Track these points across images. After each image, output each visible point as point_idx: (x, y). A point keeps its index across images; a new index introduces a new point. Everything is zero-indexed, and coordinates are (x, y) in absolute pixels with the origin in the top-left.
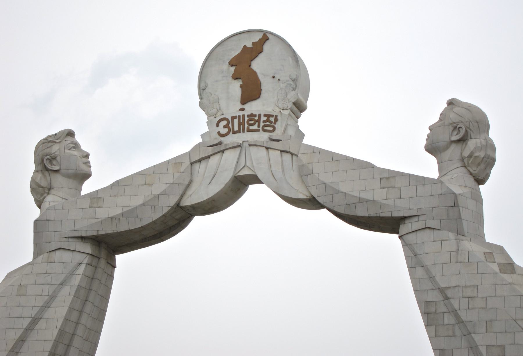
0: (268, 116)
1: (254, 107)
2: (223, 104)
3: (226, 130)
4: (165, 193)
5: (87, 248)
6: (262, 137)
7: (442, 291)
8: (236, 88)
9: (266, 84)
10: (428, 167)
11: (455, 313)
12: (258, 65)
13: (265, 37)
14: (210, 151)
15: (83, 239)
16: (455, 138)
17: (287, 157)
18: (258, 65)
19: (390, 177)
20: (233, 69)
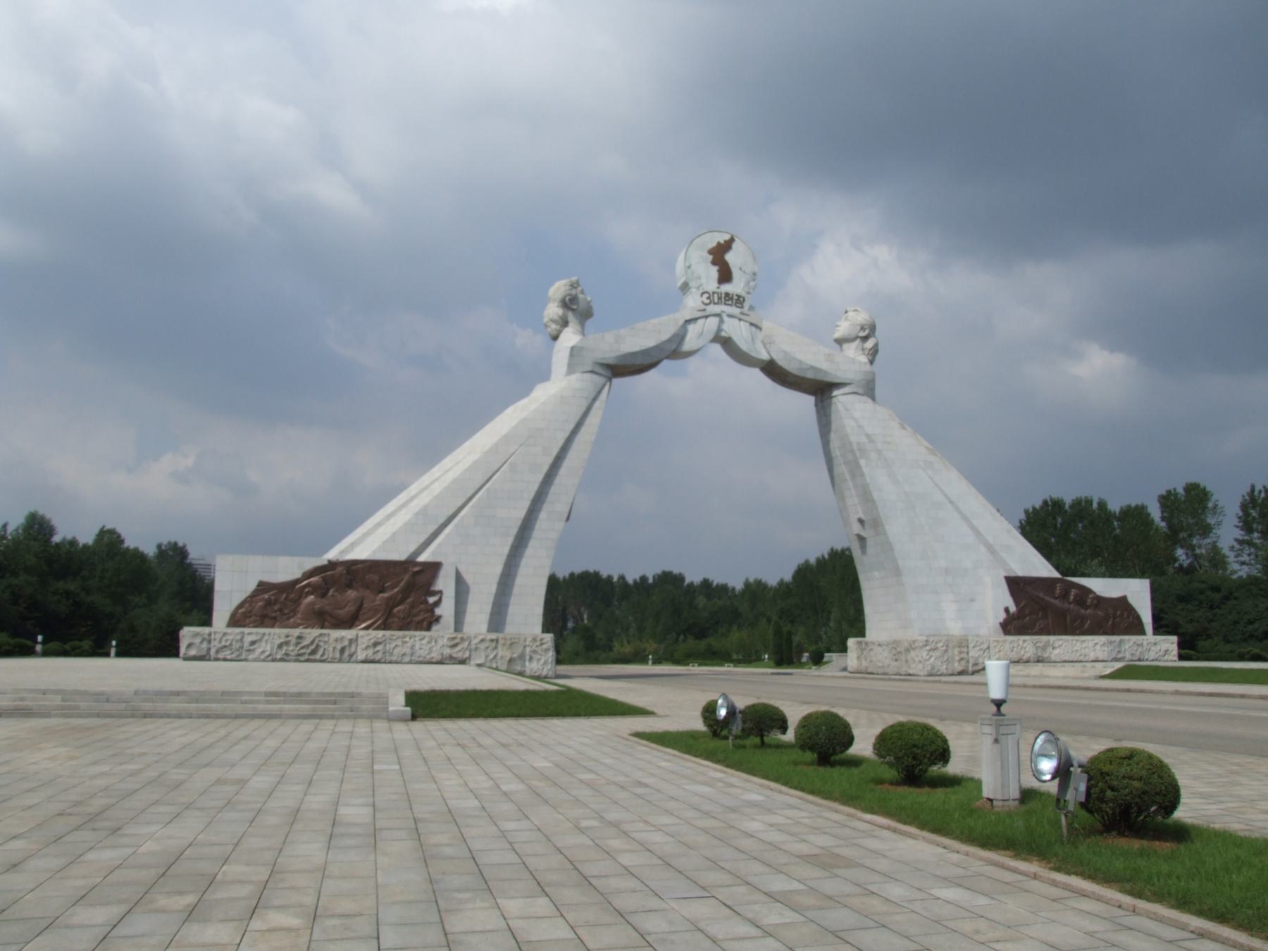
0: (739, 296)
1: (726, 288)
2: (703, 281)
4: (670, 341)
5: (608, 374)
6: (735, 310)
7: (868, 436)
8: (714, 271)
12: (729, 257)
14: (700, 314)
16: (862, 334)
18: (729, 257)
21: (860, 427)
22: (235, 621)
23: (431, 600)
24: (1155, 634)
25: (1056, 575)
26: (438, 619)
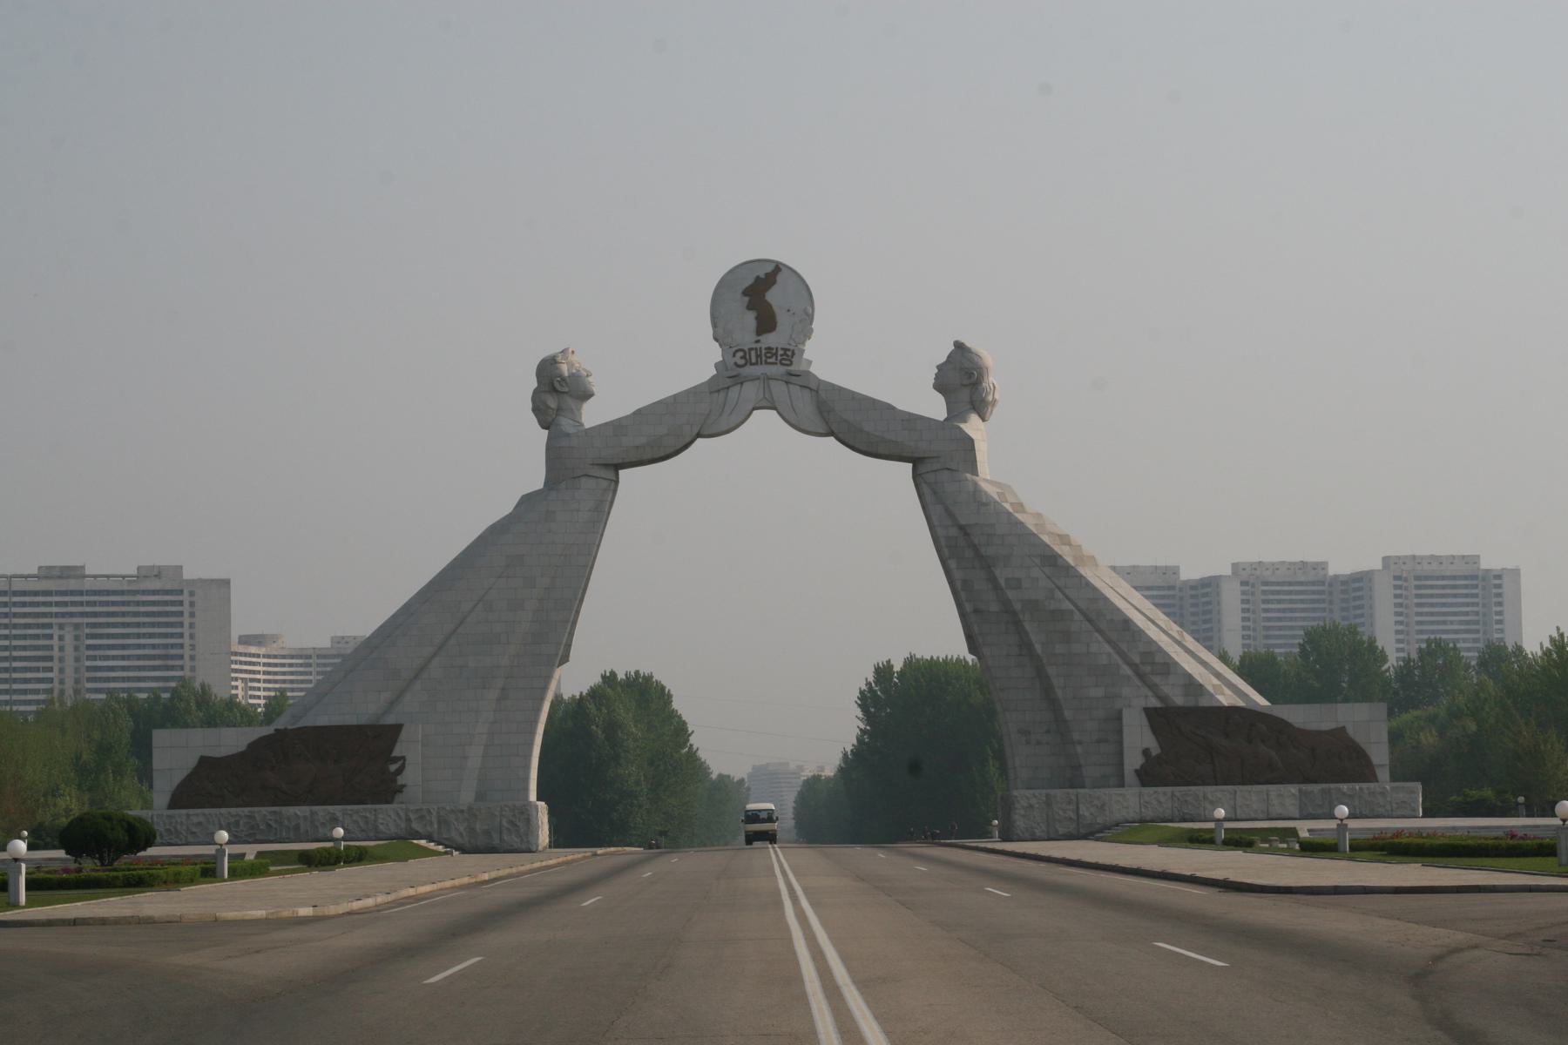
0: (786, 350)
1: (770, 340)
3: (742, 362)
5: (610, 475)
7: (962, 528)
8: (750, 319)
9: (782, 319)
10: (934, 407)
11: (975, 548)
13: (778, 267)
15: (606, 466)
17: (807, 392)
18: (773, 296)
19: (911, 420)
20: (746, 299)
21: (951, 515)
22: (175, 803)
23: (393, 768)
24: (1394, 778)
25: (1262, 701)
26: (400, 789)
